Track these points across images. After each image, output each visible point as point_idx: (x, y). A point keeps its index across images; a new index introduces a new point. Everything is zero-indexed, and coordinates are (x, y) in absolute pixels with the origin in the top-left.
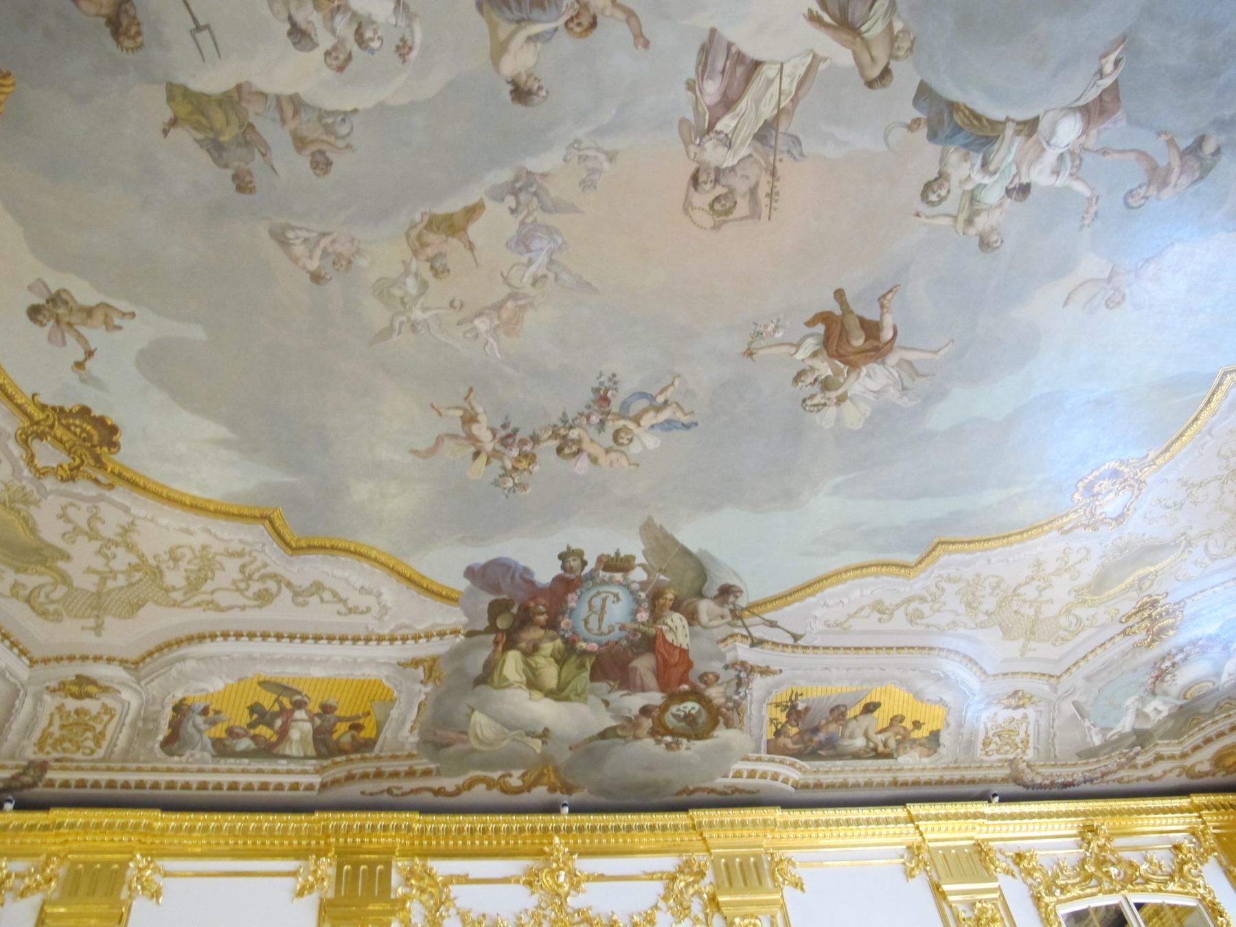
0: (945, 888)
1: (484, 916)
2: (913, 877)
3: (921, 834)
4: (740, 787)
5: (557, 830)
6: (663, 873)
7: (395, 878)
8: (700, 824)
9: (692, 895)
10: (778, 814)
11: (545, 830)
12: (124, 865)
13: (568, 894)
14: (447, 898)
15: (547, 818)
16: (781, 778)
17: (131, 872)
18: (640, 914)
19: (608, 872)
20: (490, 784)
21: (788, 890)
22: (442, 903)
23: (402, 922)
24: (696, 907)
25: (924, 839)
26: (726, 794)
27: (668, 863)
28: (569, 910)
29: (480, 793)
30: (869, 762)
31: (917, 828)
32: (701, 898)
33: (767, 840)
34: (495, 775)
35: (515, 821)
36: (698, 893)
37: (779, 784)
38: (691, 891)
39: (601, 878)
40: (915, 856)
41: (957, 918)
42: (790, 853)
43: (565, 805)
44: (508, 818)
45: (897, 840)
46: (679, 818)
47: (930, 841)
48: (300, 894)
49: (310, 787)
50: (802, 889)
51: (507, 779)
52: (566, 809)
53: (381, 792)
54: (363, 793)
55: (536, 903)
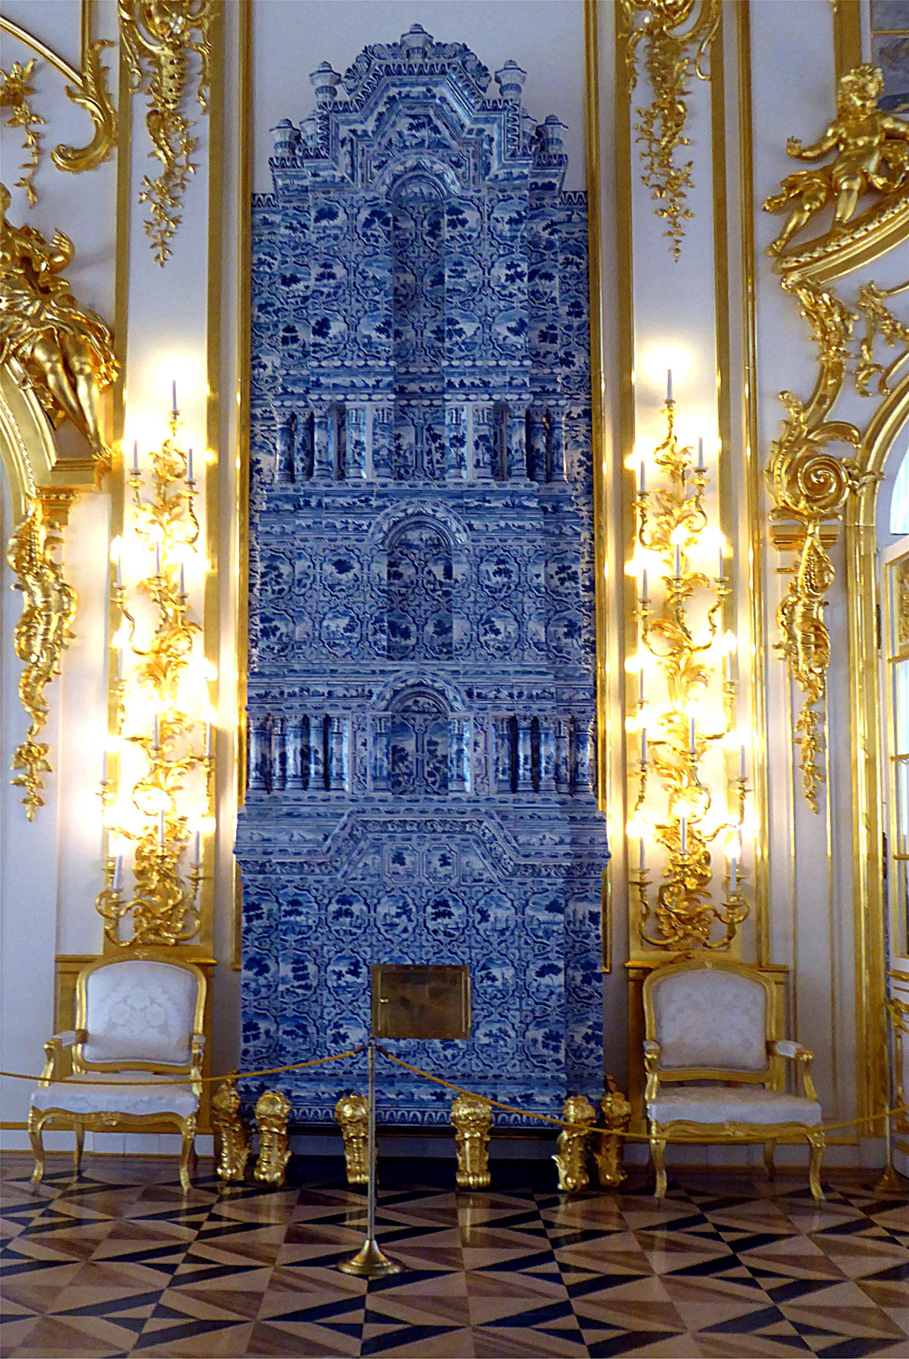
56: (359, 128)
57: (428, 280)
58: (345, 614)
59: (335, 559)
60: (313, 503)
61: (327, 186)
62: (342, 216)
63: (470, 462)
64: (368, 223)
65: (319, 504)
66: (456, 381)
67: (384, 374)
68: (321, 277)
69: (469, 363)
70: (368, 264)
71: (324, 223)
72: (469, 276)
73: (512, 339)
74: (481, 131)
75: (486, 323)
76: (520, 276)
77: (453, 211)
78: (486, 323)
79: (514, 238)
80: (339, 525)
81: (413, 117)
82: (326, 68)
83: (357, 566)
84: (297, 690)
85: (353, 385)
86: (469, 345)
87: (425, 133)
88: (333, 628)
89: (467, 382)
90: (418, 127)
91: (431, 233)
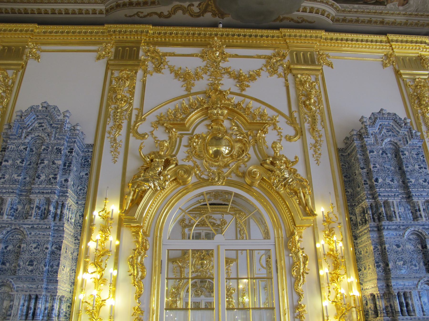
0: (402, 71)
1: (180, 68)
2: (386, 67)
3: (393, 49)
4: (305, 18)
5: (216, 35)
6: (266, 56)
7: (141, 53)
8: (285, 36)
9: (279, 66)
10: (323, 34)
11: (211, 35)
12: (24, 48)
13: (220, 61)
14: (165, 61)
15: (212, 29)
16: (326, 13)
17: (27, 51)
18: (253, 71)
19: (239, 54)
20: (185, 11)
21: (325, 68)
22: (162, 63)
23: (143, 70)
24: (280, 70)
25: (393, 52)
26: (298, 22)
27: (269, 52)
28: (220, 68)
29: (179, 16)
30: (371, 7)
31: (391, 46)
32: (283, 67)
33: (317, 45)
34: (186, 4)
35: (197, 30)
36: (282, 65)
37: (324, 18)
38: (278, 64)
39: (236, 56)
40: (388, 59)
41: (406, 85)
42: (327, 52)
43: (221, 23)
44: (194, 29)
45: (380, 51)
46: (275, 32)
47: (396, 53)
48: (98, 59)
49: (101, 12)
50: (332, 67)
51: (192, 7)
52: (221, 25)
53: (134, 15)
54: (126, 15)
55: (205, 65)
56: (375, 131)
57: (397, 169)
58: (402, 260)
59: (396, 244)
60: (386, 228)
61: (370, 145)
62: (375, 153)
63: (423, 216)
64: (382, 154)
65: (387, 228)
66: (414, 194)
67: (396, 192)
68: (374, 167)
69: (416, 190)
70: (385, 164)
71: (371, 154)
72: (410, 167)
73: (424, 183)
74: (404, 133)
75: (417, 180)
76: (422, 168)
77: (402, 152)
78: (417, 180)
79: (418, 158)
80: (395, 234)
81: (387, 129)
82: (362, 117)
83: (402, 246)
84: (395, 284)
85: (389, 195)
86: (414, 185)
87: (390, 133)
88: (399, 264)
89: (417, 194)
90: (389, 131)
91: (395, 157)
